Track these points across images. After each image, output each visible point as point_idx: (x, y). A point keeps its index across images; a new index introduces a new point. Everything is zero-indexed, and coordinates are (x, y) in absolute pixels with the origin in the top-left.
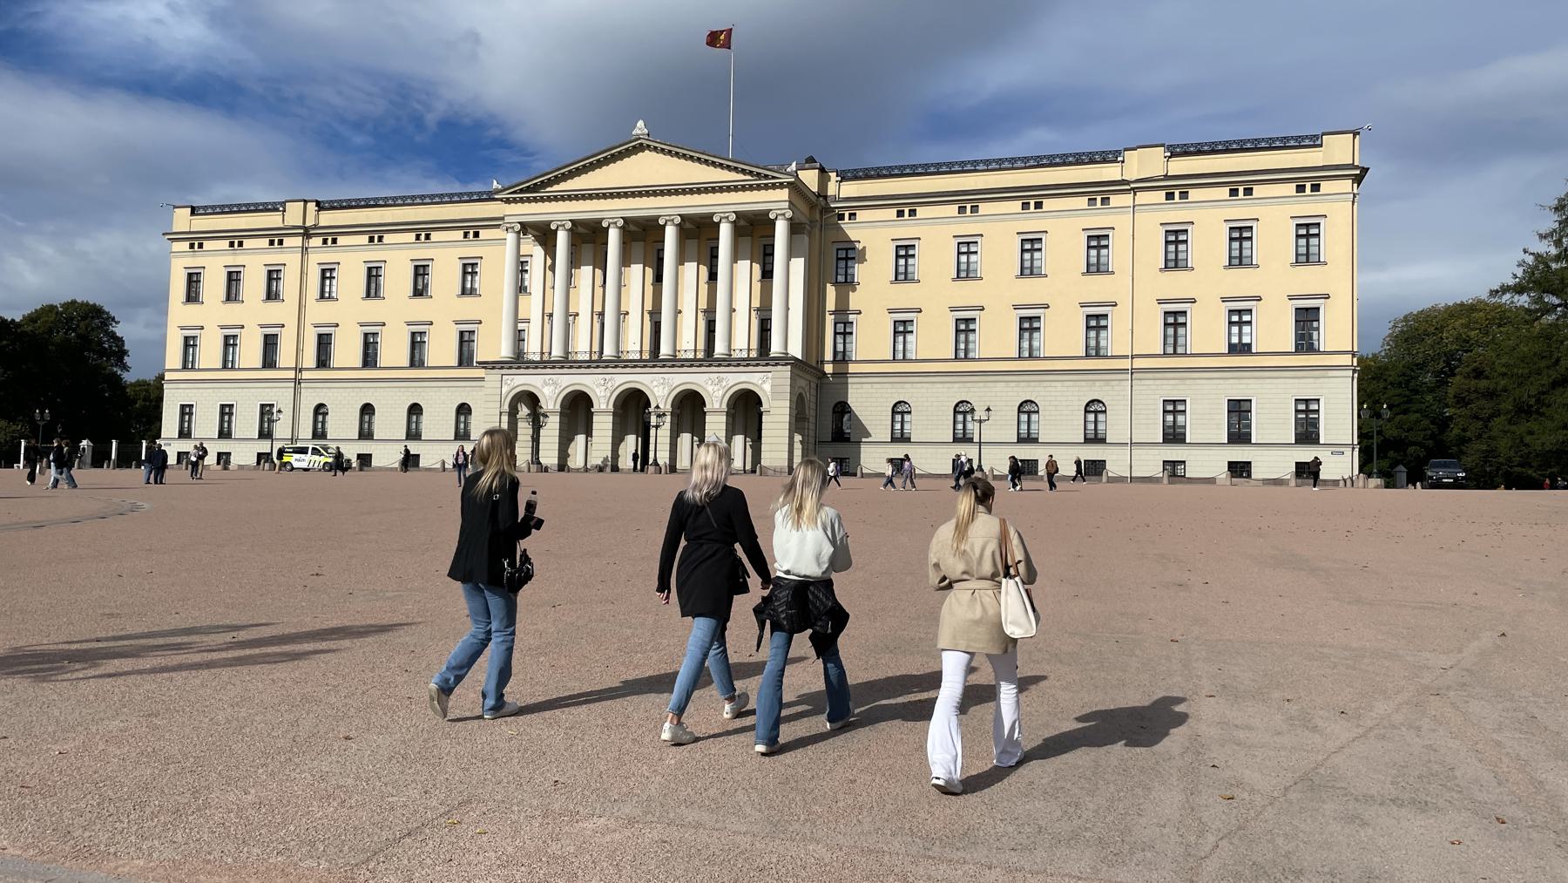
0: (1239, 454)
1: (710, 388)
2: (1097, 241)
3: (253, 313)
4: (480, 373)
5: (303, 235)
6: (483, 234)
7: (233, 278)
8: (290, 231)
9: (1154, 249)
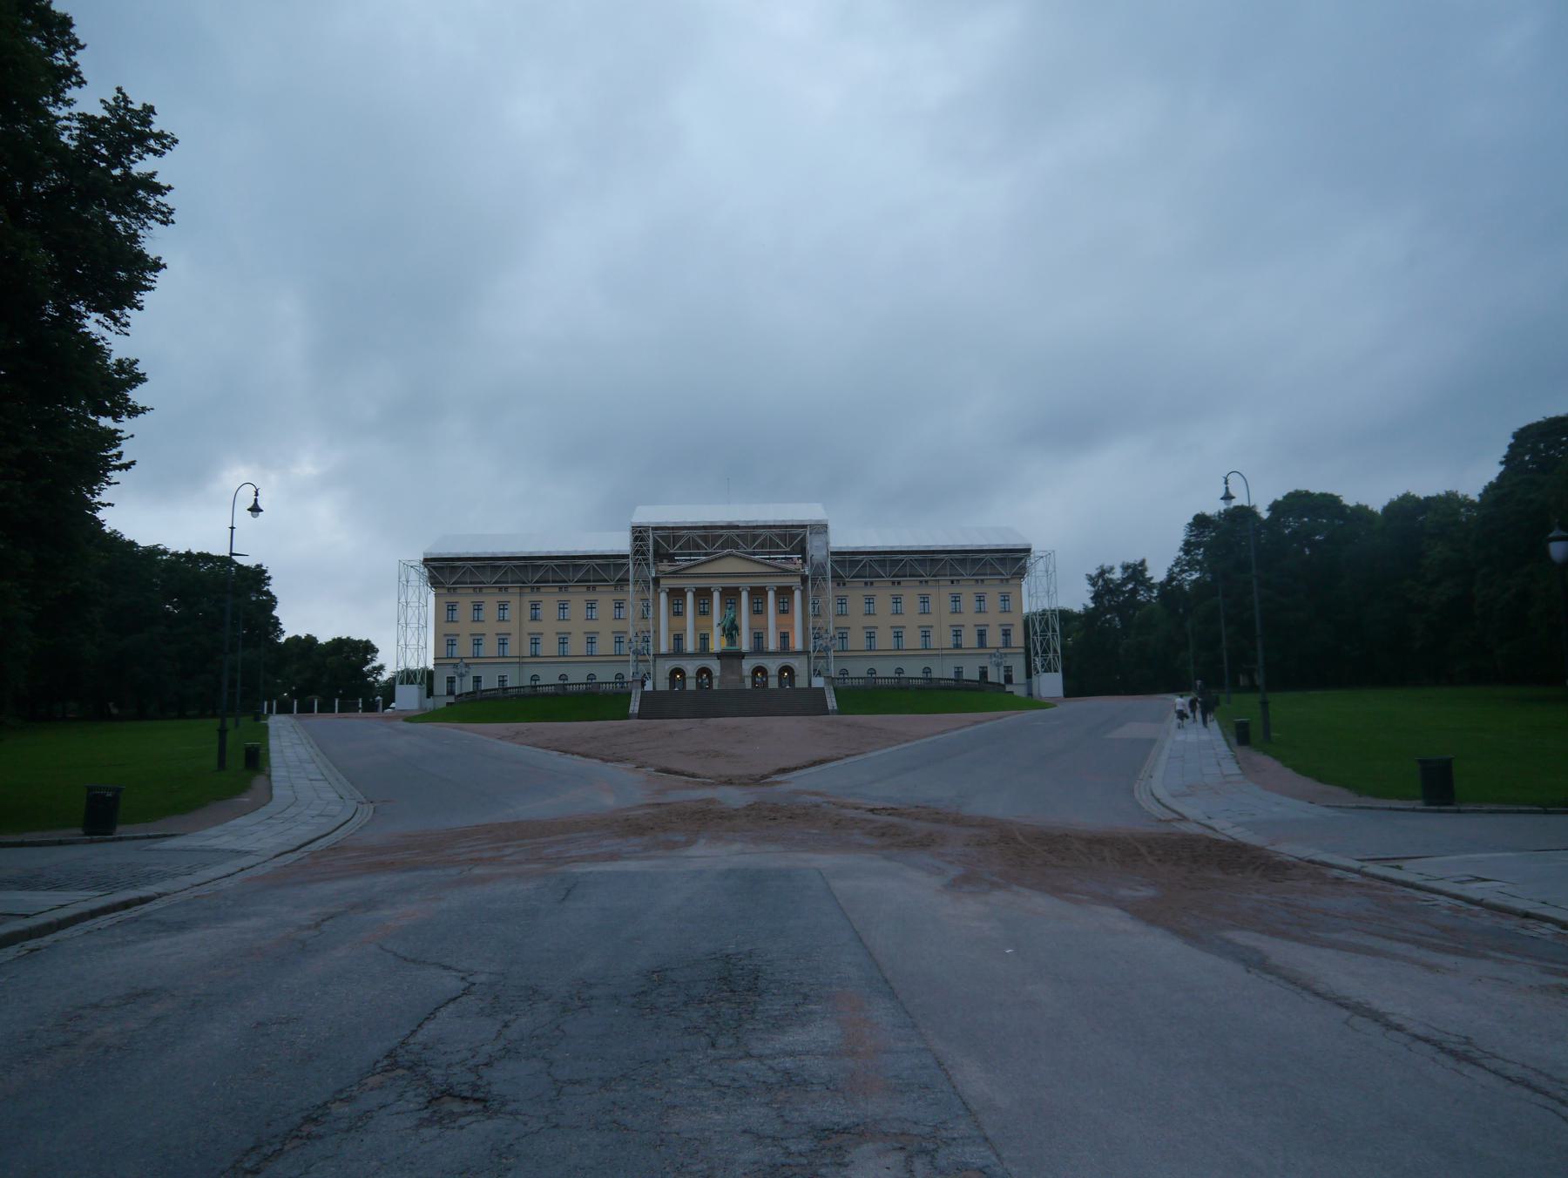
3: (490, 625)
7: (478, 607)
9: (948, 604)
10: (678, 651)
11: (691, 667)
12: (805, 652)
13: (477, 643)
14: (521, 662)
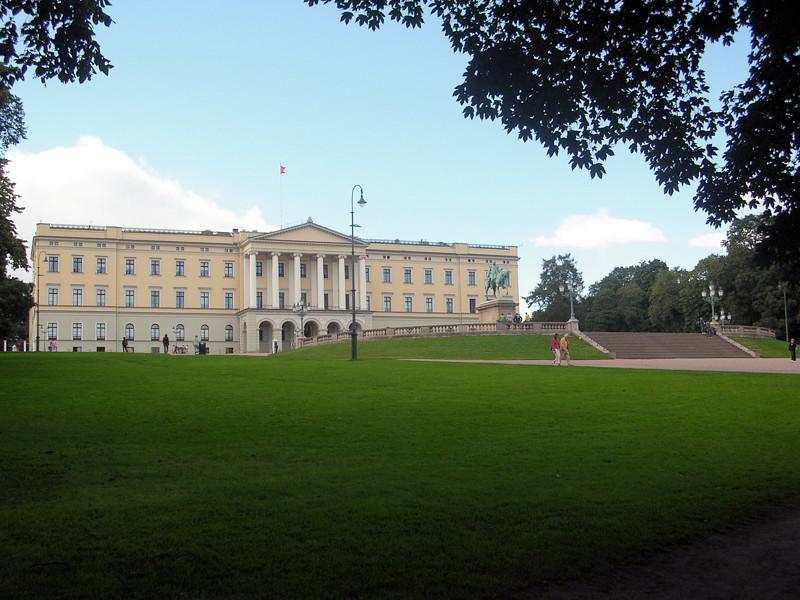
2: (449, 274)
9: (466, 278)
11: (277, 321)
12: (368, 311)
14: (117, 312)
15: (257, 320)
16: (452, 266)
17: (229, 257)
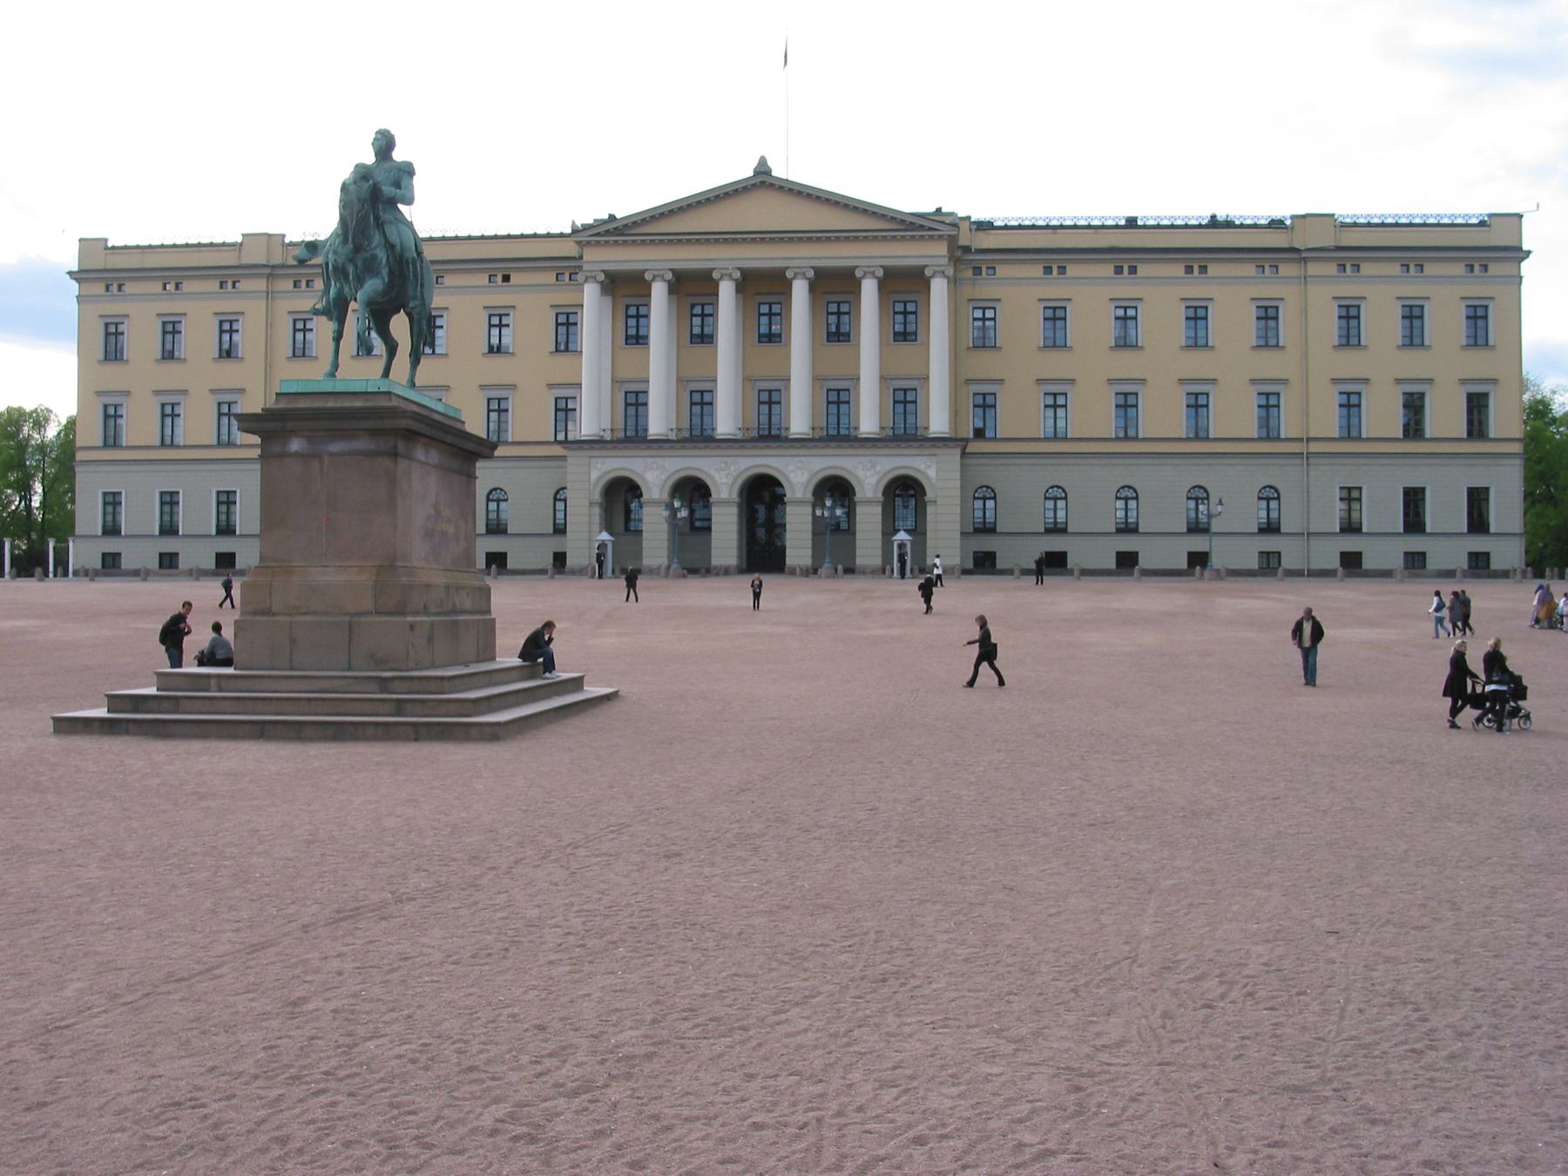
0: (1415, 543)
1: (861, 474)
2: (1268, 315)
4: (558, 450)
5: (269, 276)
6: (515, 279)
7: (171, 329)
8: (250, 270)
9: (1328, 325)
10: (633, 436)
11: (655, 476)
13: (169, 413)
15: (594, 475)
16: (1281, 288)
17: (564, 297)
